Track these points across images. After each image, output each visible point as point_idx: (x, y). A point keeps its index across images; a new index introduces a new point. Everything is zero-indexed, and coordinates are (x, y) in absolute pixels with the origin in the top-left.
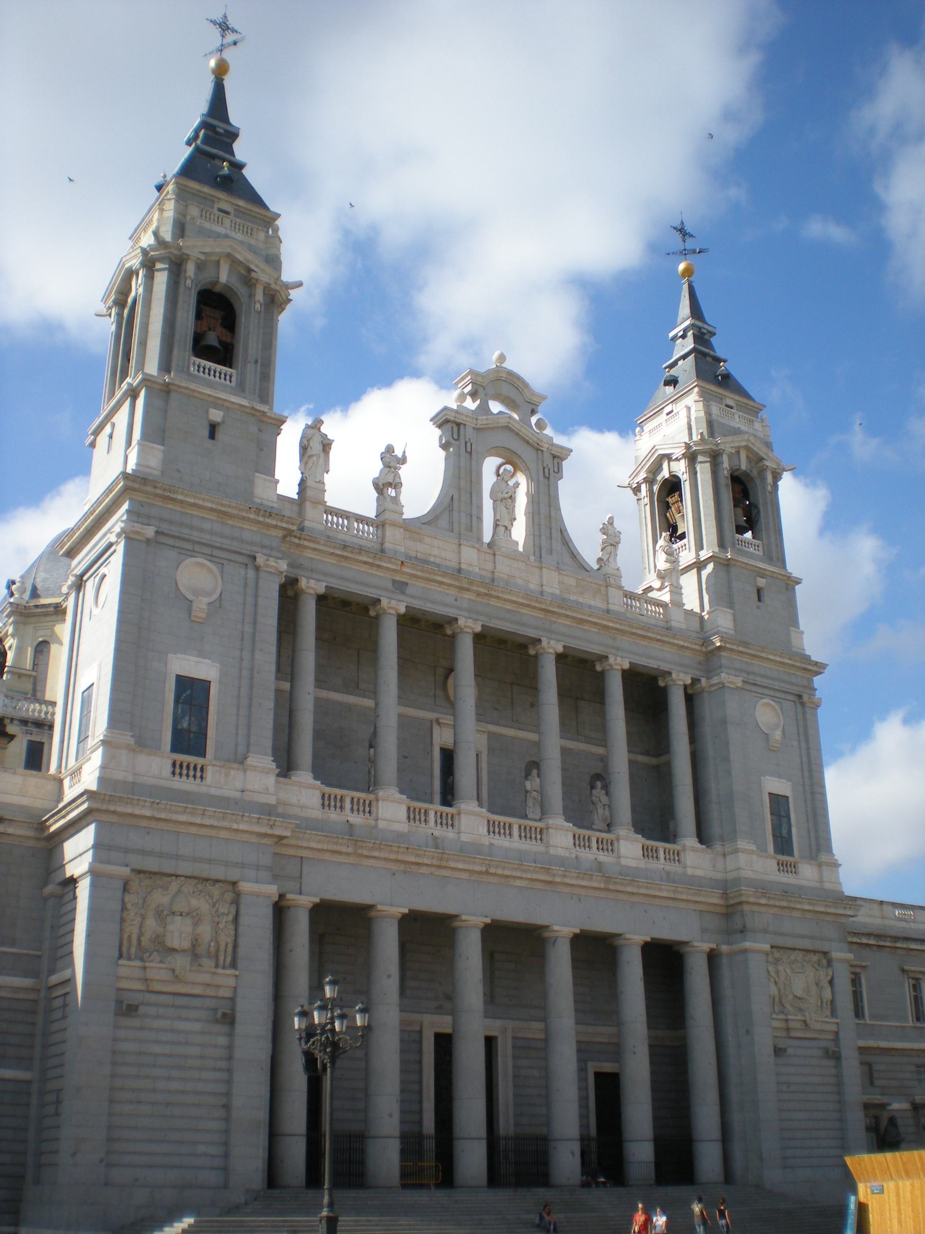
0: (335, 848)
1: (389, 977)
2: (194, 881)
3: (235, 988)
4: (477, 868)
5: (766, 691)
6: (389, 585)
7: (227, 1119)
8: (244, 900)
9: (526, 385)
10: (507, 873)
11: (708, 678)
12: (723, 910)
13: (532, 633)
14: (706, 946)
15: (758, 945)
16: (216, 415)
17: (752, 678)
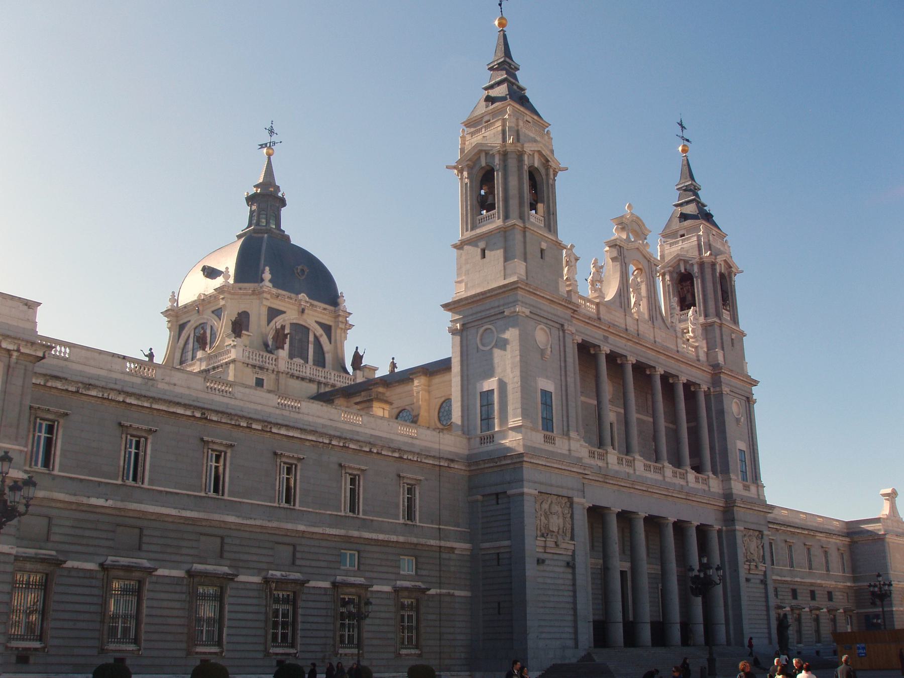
0: (597, 479)
1: (616, 543)
2: (555, 497)
3: (574, 551)
4: (644, 489)
5: (737, 395)
6: (602, 338)
7: (575, 615)
8: (575, 506)
9: (644, 225)
10: (654, 491)
11: (714, 388)
12: (721, 509)
13: (652, 364)
14: (717, 527)
15: (739, 527)
16: (544, 245)
17: (734, 390)
